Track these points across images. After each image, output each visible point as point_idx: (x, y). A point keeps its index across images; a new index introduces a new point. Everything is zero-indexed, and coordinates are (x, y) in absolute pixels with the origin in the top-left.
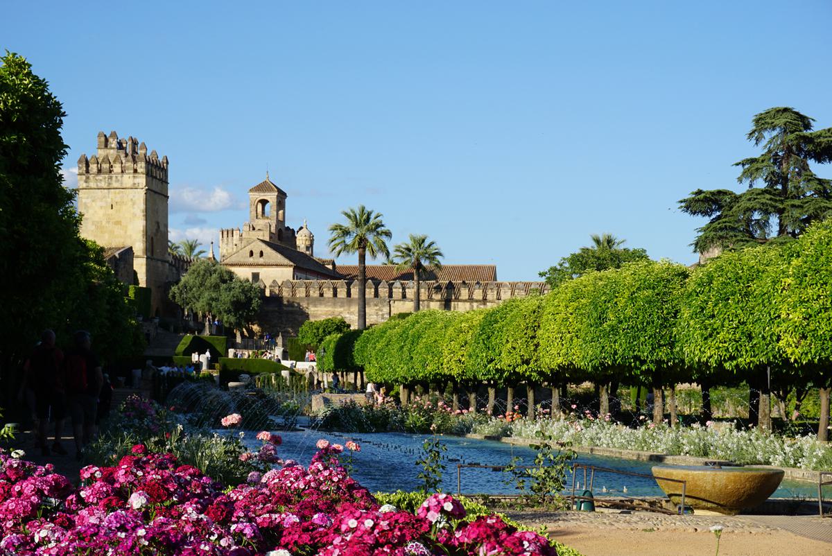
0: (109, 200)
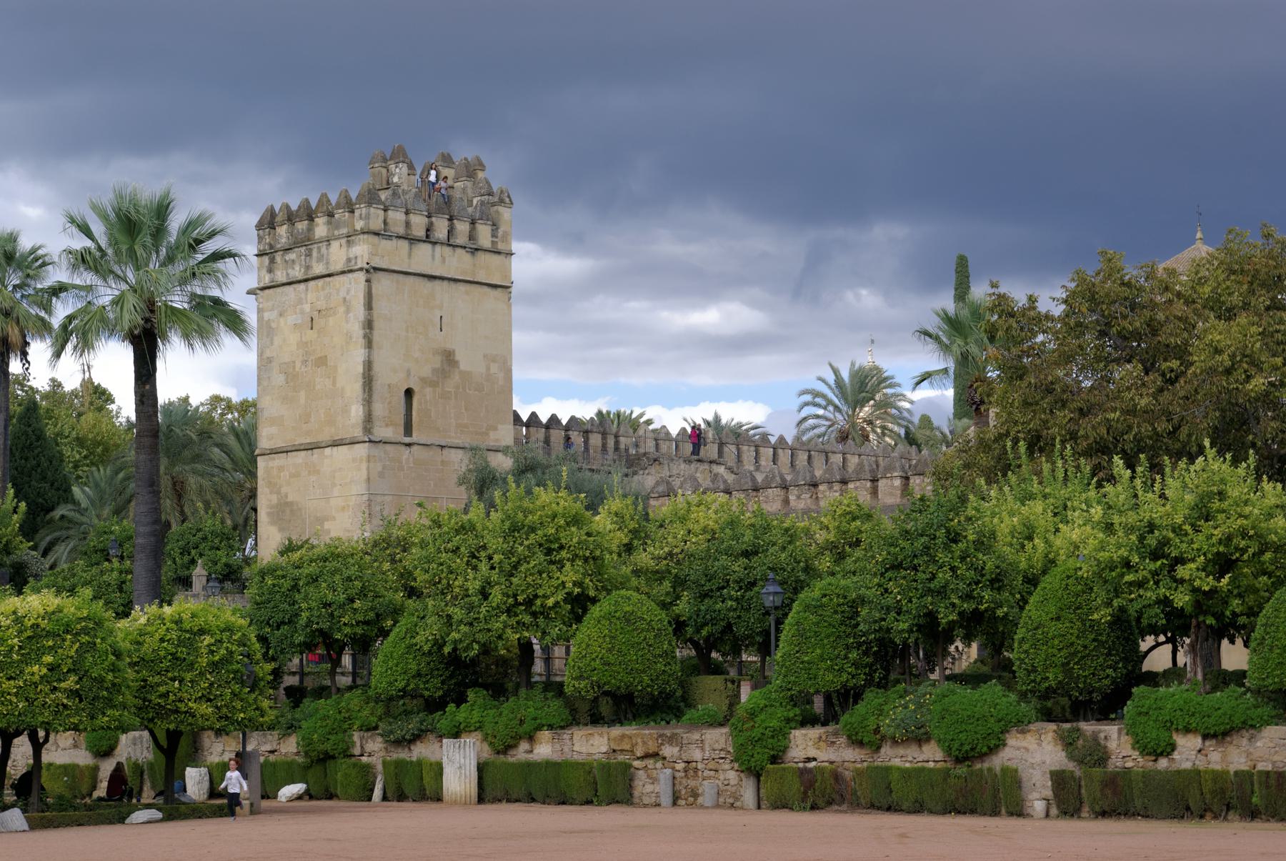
0: (307, 308)
